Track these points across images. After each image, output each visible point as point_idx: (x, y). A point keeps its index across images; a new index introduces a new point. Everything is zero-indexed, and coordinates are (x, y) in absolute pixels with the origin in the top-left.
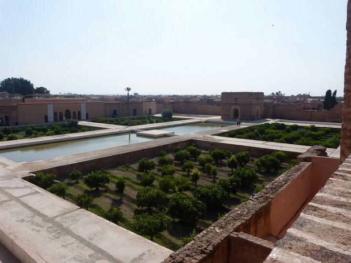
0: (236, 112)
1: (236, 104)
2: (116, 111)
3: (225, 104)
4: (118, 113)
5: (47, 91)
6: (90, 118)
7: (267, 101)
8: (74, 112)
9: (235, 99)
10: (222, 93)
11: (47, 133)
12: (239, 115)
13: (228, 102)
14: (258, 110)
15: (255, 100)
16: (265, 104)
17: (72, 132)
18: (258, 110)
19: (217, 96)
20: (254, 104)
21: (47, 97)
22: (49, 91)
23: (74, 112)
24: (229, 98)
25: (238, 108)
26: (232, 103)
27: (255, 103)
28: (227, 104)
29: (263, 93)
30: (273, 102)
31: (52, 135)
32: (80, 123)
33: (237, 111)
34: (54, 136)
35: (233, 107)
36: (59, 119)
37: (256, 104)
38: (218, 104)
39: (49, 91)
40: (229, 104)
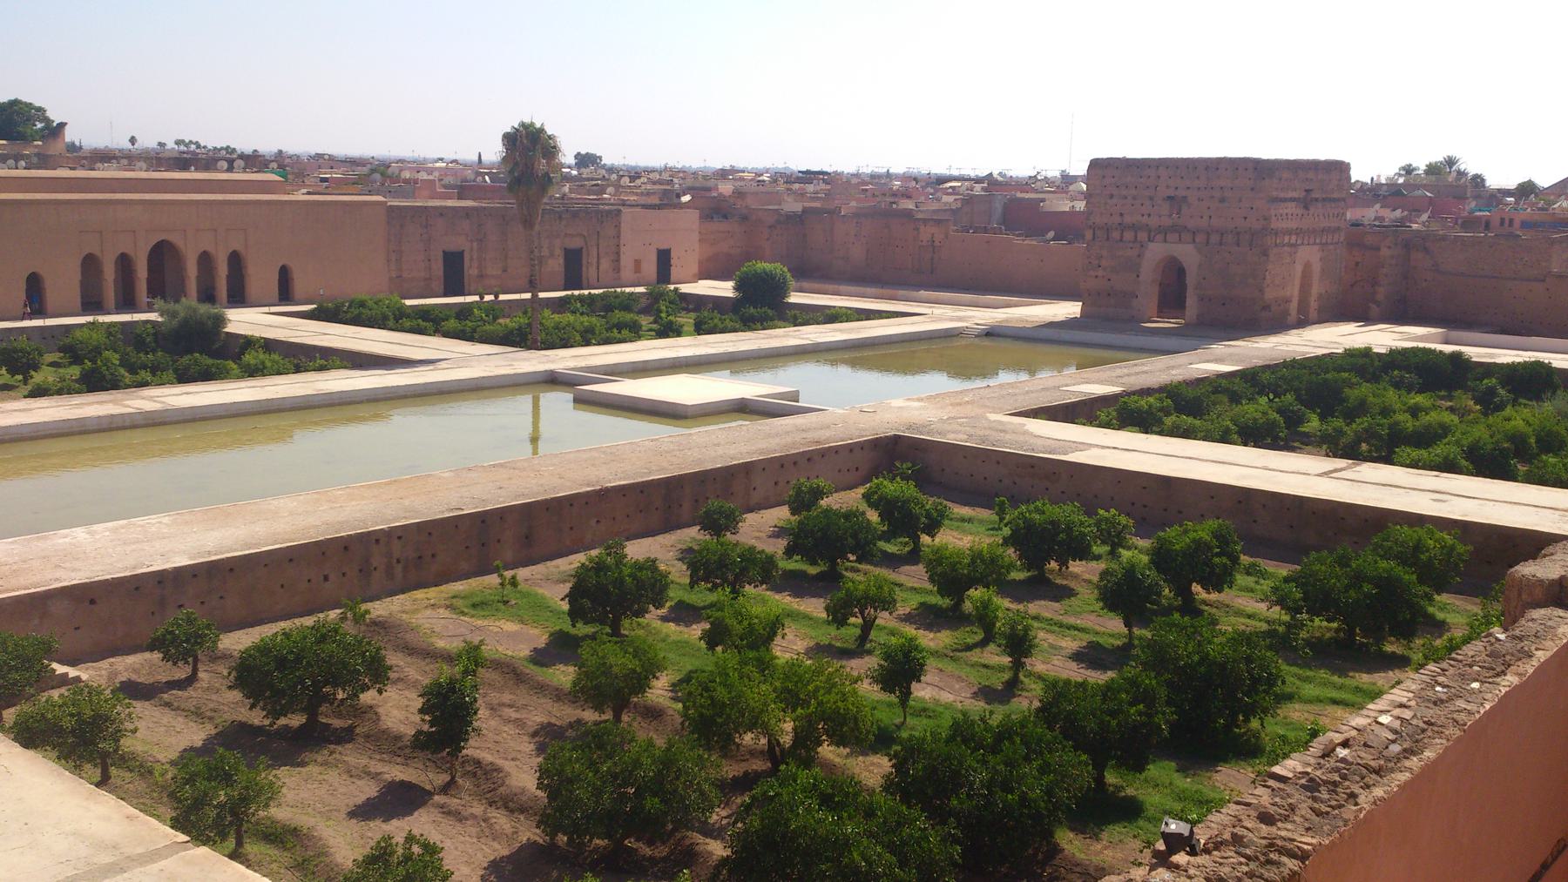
0: (1174, 275)
1: (1175, 229)
2: (462, 253)
3: (1108, 229)
4: (471, 270)
5: (48, 121)
6: (299, 286)
7: (1369, 214)
8: (205, 260)
9: (1170, 198)
10: (1095, 164)
11: (38, 378)
12: (1191, 301)
13: (1128, 219)
14: (1307, 265)
15: (1291, 208)
16: (1357, 237)
17: (184, 378)
18: (1307, 265)
19: (1067, 179)
20: (1289, 232)
21: (44, 161)
22: (62, 125)
23: (205, 260)
24: (807, 171)
25: (1187, 254)
26: (1153, 222)
27: (1292, 225)
28: (1123, 227)
29: (1341, 168)
30: (1401, 223)
31: (62, 390)
32: (244, 321)
33: (1181, 272)
34: (77, 400)
35: (1156, 251)
36: (110, 294)
37: (1298, 232)
38: (1066, 228)
39: (62, 125)
40: (1135, 228)
